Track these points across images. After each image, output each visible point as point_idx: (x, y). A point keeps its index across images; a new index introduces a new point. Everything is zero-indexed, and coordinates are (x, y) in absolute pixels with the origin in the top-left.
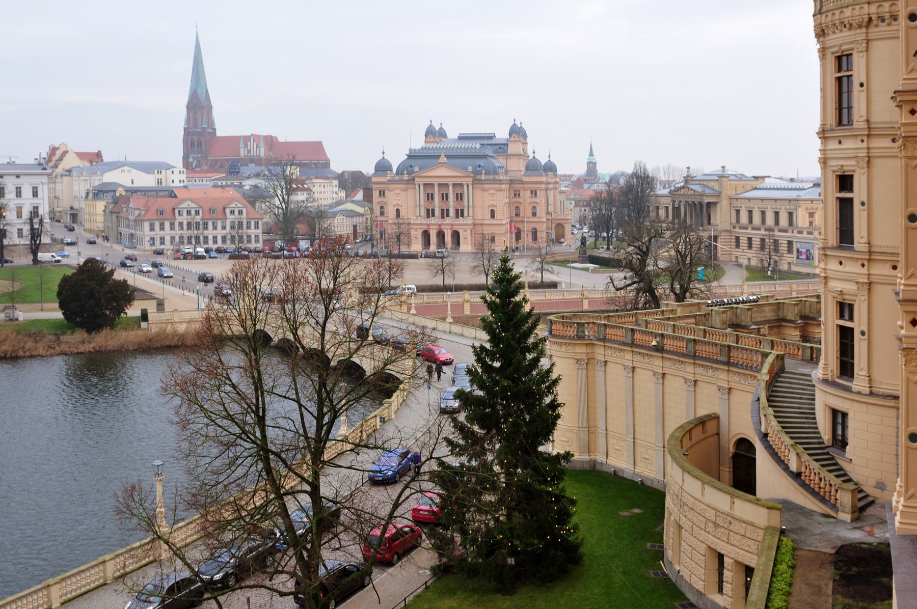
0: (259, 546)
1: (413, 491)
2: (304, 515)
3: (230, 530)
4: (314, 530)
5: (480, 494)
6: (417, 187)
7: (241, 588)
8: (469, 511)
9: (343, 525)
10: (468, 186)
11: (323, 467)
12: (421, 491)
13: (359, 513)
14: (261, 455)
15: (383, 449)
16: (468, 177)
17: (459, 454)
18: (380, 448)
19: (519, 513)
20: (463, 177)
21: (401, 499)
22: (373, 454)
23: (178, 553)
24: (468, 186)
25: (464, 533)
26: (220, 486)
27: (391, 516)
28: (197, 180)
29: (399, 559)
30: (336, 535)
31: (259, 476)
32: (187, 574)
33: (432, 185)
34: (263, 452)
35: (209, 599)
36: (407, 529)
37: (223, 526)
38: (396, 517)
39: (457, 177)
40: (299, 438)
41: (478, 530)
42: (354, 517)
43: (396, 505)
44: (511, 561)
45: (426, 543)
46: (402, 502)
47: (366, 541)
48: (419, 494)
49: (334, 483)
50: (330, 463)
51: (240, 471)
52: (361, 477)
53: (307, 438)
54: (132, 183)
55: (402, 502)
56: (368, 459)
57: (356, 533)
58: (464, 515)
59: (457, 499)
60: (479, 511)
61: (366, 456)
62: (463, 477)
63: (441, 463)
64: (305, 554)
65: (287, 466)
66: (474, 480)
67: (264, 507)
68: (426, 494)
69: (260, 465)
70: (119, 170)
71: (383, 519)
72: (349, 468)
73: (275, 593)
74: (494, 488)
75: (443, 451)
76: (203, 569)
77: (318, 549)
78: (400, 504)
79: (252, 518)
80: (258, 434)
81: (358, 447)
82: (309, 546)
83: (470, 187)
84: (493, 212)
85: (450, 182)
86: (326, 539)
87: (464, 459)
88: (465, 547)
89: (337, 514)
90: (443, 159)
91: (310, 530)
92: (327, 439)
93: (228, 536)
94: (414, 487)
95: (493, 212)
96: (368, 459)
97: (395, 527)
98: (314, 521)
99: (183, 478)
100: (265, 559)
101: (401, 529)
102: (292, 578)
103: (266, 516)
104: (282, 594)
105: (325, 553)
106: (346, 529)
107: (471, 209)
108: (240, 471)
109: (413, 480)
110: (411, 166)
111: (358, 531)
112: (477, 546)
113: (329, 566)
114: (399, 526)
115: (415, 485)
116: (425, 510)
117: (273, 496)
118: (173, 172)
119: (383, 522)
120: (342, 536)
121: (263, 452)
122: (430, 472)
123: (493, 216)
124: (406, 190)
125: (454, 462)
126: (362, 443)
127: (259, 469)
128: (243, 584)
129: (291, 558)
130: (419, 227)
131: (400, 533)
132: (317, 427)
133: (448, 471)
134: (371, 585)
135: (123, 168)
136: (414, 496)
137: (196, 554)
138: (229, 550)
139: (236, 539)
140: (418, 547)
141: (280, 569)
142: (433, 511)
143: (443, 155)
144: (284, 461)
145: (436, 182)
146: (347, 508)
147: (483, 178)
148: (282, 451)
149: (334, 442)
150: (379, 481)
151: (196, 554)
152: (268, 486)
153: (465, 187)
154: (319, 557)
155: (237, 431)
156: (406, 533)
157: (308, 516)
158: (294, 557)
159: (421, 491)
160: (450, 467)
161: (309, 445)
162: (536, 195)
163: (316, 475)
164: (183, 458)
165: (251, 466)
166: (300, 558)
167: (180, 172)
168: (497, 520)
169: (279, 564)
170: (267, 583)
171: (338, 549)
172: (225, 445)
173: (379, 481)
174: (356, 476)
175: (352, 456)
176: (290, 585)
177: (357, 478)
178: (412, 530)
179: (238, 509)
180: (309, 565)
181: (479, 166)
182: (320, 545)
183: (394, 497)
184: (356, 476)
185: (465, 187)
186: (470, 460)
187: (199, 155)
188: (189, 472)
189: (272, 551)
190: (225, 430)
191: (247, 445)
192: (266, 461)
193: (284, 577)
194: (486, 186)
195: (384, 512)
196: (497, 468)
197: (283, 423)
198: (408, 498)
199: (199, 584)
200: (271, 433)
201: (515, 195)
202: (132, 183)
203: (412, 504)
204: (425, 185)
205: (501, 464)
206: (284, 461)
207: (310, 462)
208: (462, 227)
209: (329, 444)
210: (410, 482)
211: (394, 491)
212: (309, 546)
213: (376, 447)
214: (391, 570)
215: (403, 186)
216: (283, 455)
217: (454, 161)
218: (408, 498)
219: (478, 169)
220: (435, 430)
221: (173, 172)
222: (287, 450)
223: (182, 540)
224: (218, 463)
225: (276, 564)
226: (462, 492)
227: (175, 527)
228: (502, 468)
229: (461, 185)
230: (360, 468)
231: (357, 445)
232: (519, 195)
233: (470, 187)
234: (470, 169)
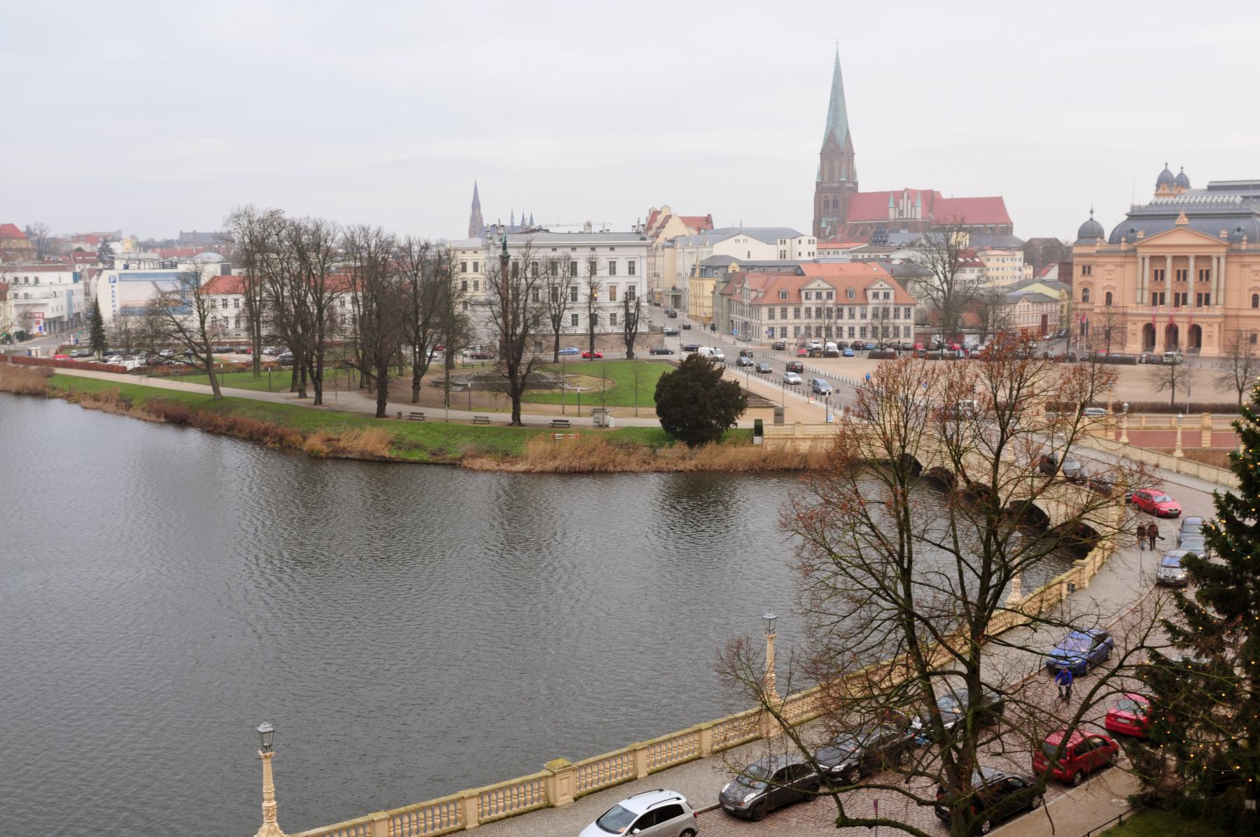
2: (956, 704)
3: (858, 711)
4: (969, 726)
5: (1212, 704)
7: (868, 787)
9: (1008, 723)
11: (985, 643)
12: (1123, 691)
13: (1032, 711)
14: (903, 620)
15: (1072, 627)
17: (1182, 646)
18: (1068, 625)
21: (1095, 698)
22: (1057, 633)
23: (789, 731)
25: (1182, 755)
26: (848, 655)
28: (831, 251)
29: (1085, 778)
30: (998, 736)
31: (899, 646)
32: (800, 759)
34: (906, 614)
35: (826, 794)
36: (1097, 740)
37: (849, 705)
38: (1084, 722)
40: (955, 602)
41: (1202, 755)
42: (1024, 715)
44: (1251, 804)
46: (1094, 703)
47: (1039, 749)
48: (1120, 694)
49: (1000, 667)
50: (995, 639)
51: (876, 637)
52: (1038, 663)
53: (966, 603)
54: (749, 257)
55: (1094, 703)
56: (1048, 639)
58: (1184, 730)
59: (1176, 707)
60: (1208, 727)
61: (1046, 634)
62: (1186, 677)
63: (1155, 655)
64: (954, 754)
65: (936, 637)
66: (1202, 684)
67: (903, 687)
69: (902, 632)
71: (1066, 723)
72: (1022, 648)
73: (911, 800)
74: (1233, 698)
75: (1159, 639)
76: (821, 756)
78: (1091, 706)
79: (888, 699)
80: (901, 591)
81: (1035, 621)
82: (960, 745)
87: (1190, 653)
88: (1182, 776)
89: (999, 707)
92: (994, 607)
93: (855, 719)
96: (1048, 639)
97: (1082, 735)
98: (970, 714)
99: (803, 642)
100: (901, 753)
102: (936, 783)
103: (905, 700)
104: (921, 803)
105: (982, 758)
108: (876, 637)
109: (1113, 674)
112: (1200, 777)
113: (988, 774)
115: (1115, 682)
117: (916, 674)
119: (1066, 727)
120: (1005, 737)
121: (906, 614)
122: (1137, 667)
125: (1174, 655)
126: (1042, 617)
127: (900, 639)
128: (871, 783)
129: (935, 758)
131: (1086, 744)
132: (981, 590)
133: (1166, 668)
134: (1042, 807)
135: (737, 237)
136: (1113, 697)
137: (814, 736)
141: (921, 769)
142: (1138, 721)
144: (933, 631)
146: (1016, 702)
148: (931, 617)
149: (1002, 611)
151: (814, 736)
152: (910, 661)
154: (975, 761)
155: (875, 585)
156: (1096, 745)
158: (940, 757)
159: (1123, 691)
160: (1167, 662)
161: (968, 613)
163: (976, 653)
164: (802, 613)
165: (890, 632)
166: (948, 760)
168: (1234, 744)
169: (919, 763)
170: (903, 785)
171: (999, 754)
172: (857, 601)
174: (1032, 661)
175: (1027, 633)
176: (932, 792)
180: (960, 770)
182: (976, 746)
186: (1198, 656)
187: (835, 219)
188: (810, 631)
189: (910, 746)
190: (858, 582)
191: (883, 603)
192: (910, 628)
193: (924, 781)
196: (1238, 671)
197: (935, 580)
198: (1103, 698)
199: (814, 774)
200: (917, 592)
202: (749, 257)
205: (1246, 665)
206: (933, 631)
207: (968, 635)
209: (995, 613)
210: (1108, 677)
212: (960, 745)
213: (1062, 624)
214: (1071, 792)
216: (932, 623)
218: (1103, 698)
220: (1149, 608)
222: (939, 616)
223: (796, 716)
224: (848, 623)
225: (915, 763)
226: (1185, 700)
227: (789, 698)
228: (1247, 672)
230: (1038, 650)
231: (1035, 619)
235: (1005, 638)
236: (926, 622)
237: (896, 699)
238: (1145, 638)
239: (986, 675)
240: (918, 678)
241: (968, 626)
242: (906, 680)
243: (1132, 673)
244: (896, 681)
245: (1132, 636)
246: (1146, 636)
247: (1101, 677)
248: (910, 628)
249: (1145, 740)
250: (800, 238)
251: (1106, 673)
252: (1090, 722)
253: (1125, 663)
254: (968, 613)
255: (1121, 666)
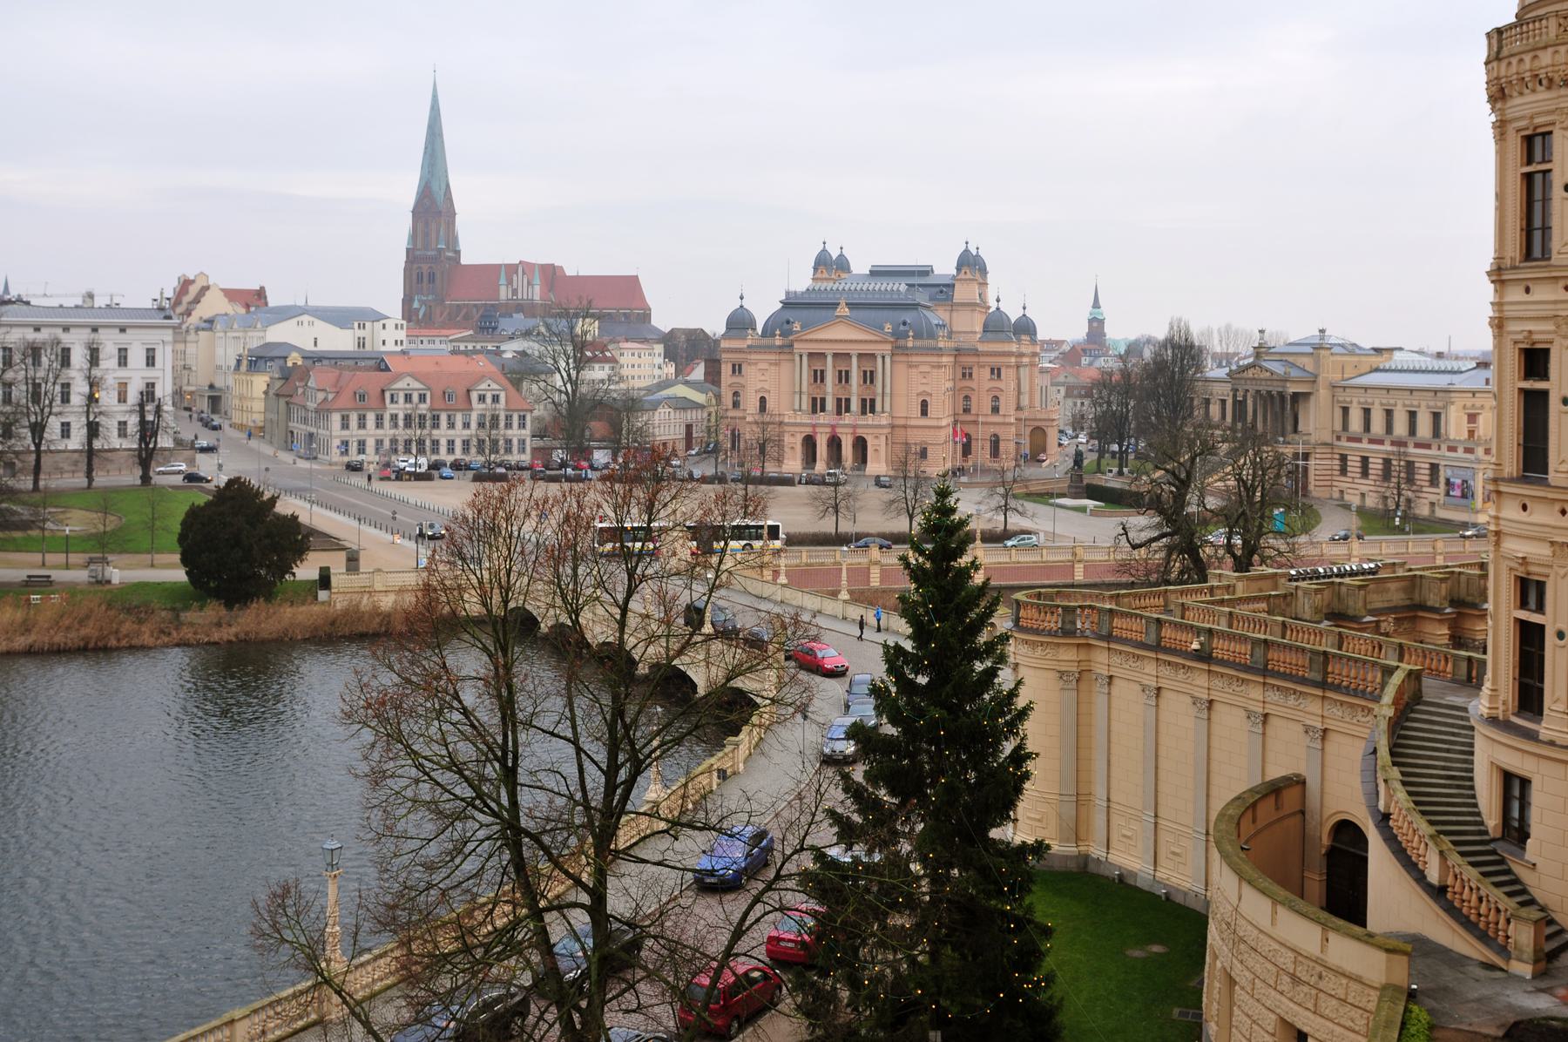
0: (497, 1000)
1: (768, 908)
2: (577, 946)
5: (886, 915)
6: (797, 358)
8: (864, 943)
10: (883, 357)
11: (613, 861)
12: (782, 909)
13: (674, 947)
16: (886, 342)
18: (714, 829)
19: (953, 950)
20: (876, 342)
21: (747, 923)
22: (702, 839)
24: (883, 357)
25: (854, 983)
27: (728, 953)
28: (425, 340)
29: (741, 1029)
30: (631, 986)
31: (503, 874)
33: (823, 356)
36: (756, 974)
38: (737, 955)
39: (866, 341)
40: (573, 809)
41: (878, 979)
42: (666, 952)
43: (738, 934)
45: (787, 1003)
46: (748, 929)
47: (682, 996)
48: (778, 914)
49: (633, 891)
50: (627, 854)
53: (587, 808)
55: (748, 929)
56: (692, 849)
57: (667, 983)
58: (856, 950)
60: (882, 945)
61: (689, 842)
62: (855, 880)
63: (820, 855)
64: (576, 1017)
65: (551, 858)
66: (875, 889)
68: (789, 913)
69: (507, 856)
70: (295, 321)
74: (912, 903)
75: (824, 835)
77: (599, 1012)
78: (744, 932)
79: (486, 952)
80: (505, 801)
81: (677, 826)
82: (584, 1004)
83: (888, 360)
84: (924, 405)
85: (854, 350)
86: (614, 992)
89: (636, 945)
90: (843, 311)
91: (585, 975)
92: (623, 812)
94: (771, 902)
95: (924, 405)
96: (692, 849)
98: (595, 960)
100: (507, 1027)
101: (746, 974)
103: (514, 948)
105: (611, 1018)
106: (651, 976)
107: (887, 399)
109: (769, 888)
110: (788, 322)
111: (670, 979)
114: (741, 970)
115: (773, 898)
116: (790, 941)
119: (714, 964)
120: (642, 987)
121: (512, 832)
122: (799, 874)
123: (924, 412)
124: (777, 364)
126: (684, 820)
127: (505, 863)
129: (551, 1026)
130: (797, 429)
133: (830, 874)
136: (771, 917)
138: (447, 1008)
139: (458, 988)
140: (770, 1009)
142: (803, 943)
143: (843, 302)
145: (830, 350)
146: (655, 937)
147: (910, 344)
148: (545, 831)
150: (711, 885)
152: (518, 895)
153: (879, 360)
156: (755, 981)
157: (583, 949)
158: (557, 1026)
159: (782, 909)
160: (834, 864)
161: (591, 821)
162: (999, 375)
163: (601, 875)
165: (490, 857)
167: (396, 326)
168: (912, 961)
171: (634, 1011)
173: (711, 885)
174: (670, 878)
175: (665, 842)
177: (672, 883)
178: (765, 977)
179: (464, 933)
181: (904, 323)
182: (604, 1002)
183: (736, 917)
184: (670, 878)
185: (879, 360)
186: (870, 852)
187: (430, 298)
192: (516, 848)
194: (914, 359)
195: (715, 948)
196: (915, 867)
197: (550, 781)
198: (758, 920)
200: (525, 798)
201: (964, 375)
203: (765, 930)
204: (811, 355)
205: (924, 860)
208: (871, 431)
209: (624, 819)
211: (735, 905)
212: (584, 1004)
213: (706, 827)
215: (773, 357)
216: (546, 839)
217: (857, 314)
218: (758, 920)
219: (902, 328)
220: (810, 799)
222: (552, 830)
225: (525, 1037)
226: (855, 912)
228: (925, 868)
229: (873, 356)
230: (679, 865)
231: (675, 823)
232: (971, 375)
233: (888, 360)
234: (888, 328)
235: (636, 852)
236: (536, 838)
237: (498, 949)
238: (804, 837)
239: (617, 905)
240: (527, 917)
241: (590, 840)
242: (510, 922)
243: (791, 884)
244: (499, 923)
245: (789, 837)
246: (806, 834)
247: (754, 892)
248: (516, 848)
249: (811, 967)
250: (382, 322)
251: (761, 886)
252: (745, 955)
253: (783, 873)
254: (591, 821)
255: (778, 877)
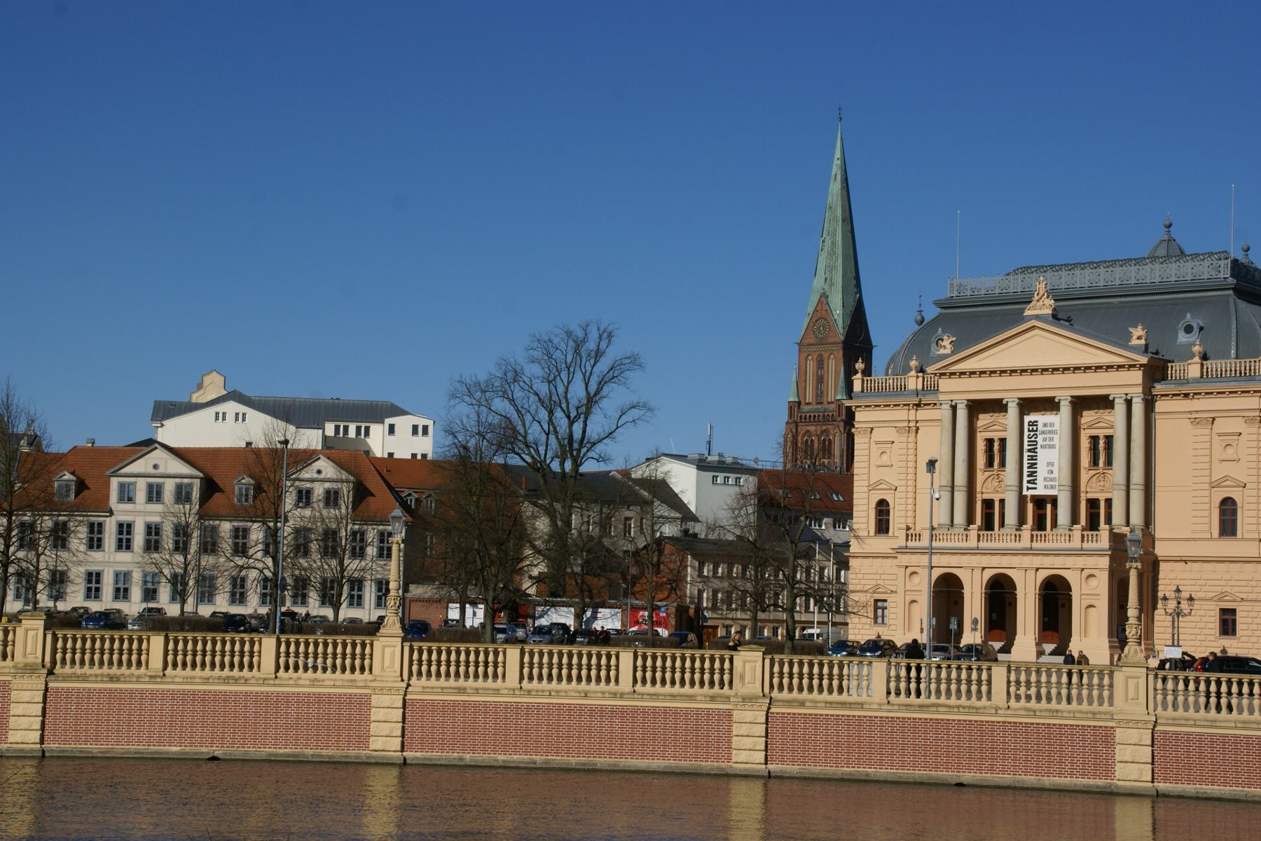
6: (946, 413)
24: (1129, 403)
33: (997, 406)
84: (1228, 509)
85: (1064, 388)
95: (1228, 509)
118: (392, 429)
123: (1228, 526)
145: (1011, 390)
153: (1120, 407)
167: (415, 429)
208: (1080, 562)
215: (901, 414)
221: (392, 429)
229: (1104, 402)
